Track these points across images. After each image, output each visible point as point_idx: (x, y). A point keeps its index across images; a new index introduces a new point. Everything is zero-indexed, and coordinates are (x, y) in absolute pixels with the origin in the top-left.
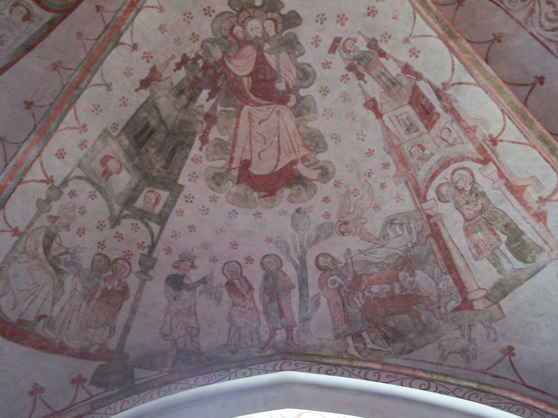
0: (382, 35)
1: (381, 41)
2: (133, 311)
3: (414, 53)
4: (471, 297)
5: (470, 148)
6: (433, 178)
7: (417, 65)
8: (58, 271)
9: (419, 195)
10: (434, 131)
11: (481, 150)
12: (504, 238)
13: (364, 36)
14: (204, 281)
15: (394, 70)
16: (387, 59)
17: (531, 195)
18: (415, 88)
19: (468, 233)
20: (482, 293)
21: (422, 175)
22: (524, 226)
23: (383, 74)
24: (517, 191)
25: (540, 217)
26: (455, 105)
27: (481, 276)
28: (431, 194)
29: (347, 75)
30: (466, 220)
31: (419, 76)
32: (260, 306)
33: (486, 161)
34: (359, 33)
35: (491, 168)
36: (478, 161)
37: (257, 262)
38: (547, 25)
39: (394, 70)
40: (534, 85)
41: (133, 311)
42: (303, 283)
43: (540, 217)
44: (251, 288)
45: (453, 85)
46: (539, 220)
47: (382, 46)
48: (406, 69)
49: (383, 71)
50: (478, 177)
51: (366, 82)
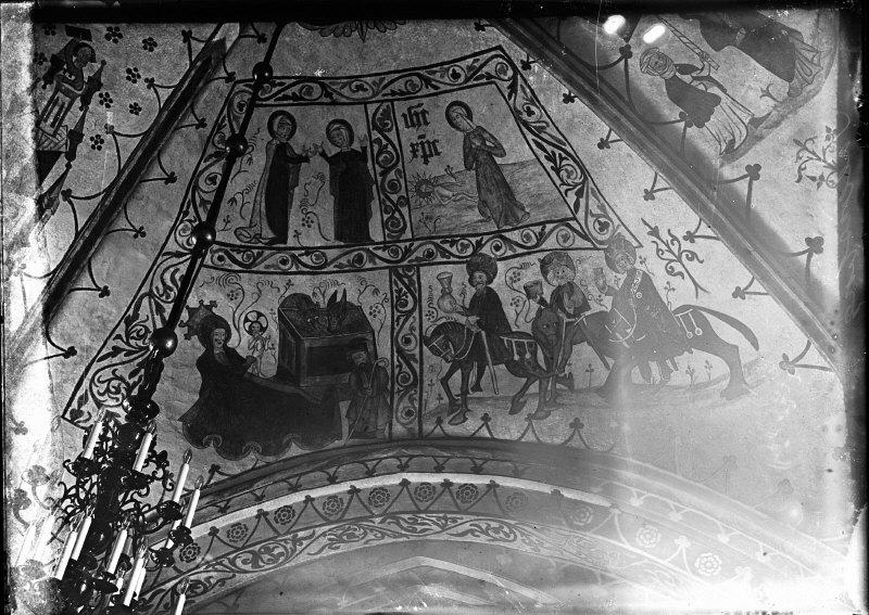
0: (107, 94)
1: (101, 95)
3: (98, 142)
7: (83, 149)
13: (101, 70)
15: (70, 121)
16: (81, 109)
18: (57, 155)
23: (62, 106)
26: (48, 212)
29: (45, 60)
31: (71, 155)
34: (104, 63)
38: (167, 276)
39: (70, 121)
40: (99, 289)
45: (71, 203)
47: (96, 97)
48: (76, 136)
49: (66, 106)
51: (44, 87)
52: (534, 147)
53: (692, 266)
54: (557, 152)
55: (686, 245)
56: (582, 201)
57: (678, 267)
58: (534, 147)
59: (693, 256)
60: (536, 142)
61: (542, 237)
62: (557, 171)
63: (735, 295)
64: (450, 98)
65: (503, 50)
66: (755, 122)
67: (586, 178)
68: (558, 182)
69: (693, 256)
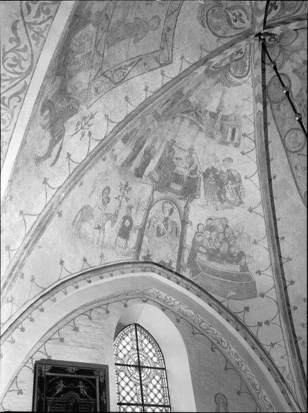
52: (133, 60)
53: (79, 134)
54: (127, 72)
55: (87, 133)
56: (107, 80)
57: (79, 127)
58: (133, 60)
59: (83, 135)
60: (133, 63)
61: (99, 53)
62: (119, 69)
63: (68, 154)
64: (162, 22)
65: (170, 63)
66: (115, 158)
67: (115, 84)
68: (116, 68)
69: (83, 135)
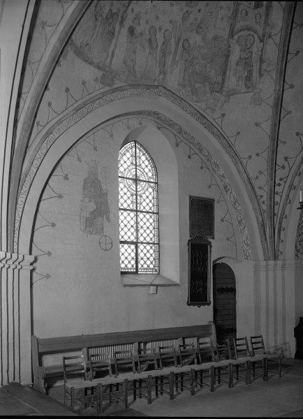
2: (115, 46)
4: (224, 89)
5: (260, 31)
6: (241, 30)
8: (96, 19)
9: (232, 35)
10: (256, 11)
11: (264, 36)
12: (246, 74)
14: (141, 34)
17: (264, 66)
19: (237, 64)
20: (227, 90)
21: (238, 26)
22: (254, 74)
24: (261, 61)
25: (261, 75)
27: (232, 82)
28: (236, 37)
30: (240, 58)
32: (158, 60)
33: (262, 41)
35: (262, 44)
36: (260, 38)
37: (163, 31)
41: (115, 46)
42: (175, 54)
43: (261, 75)
44: (157, 46)
46: (259, 76)
50: (255, 44)
